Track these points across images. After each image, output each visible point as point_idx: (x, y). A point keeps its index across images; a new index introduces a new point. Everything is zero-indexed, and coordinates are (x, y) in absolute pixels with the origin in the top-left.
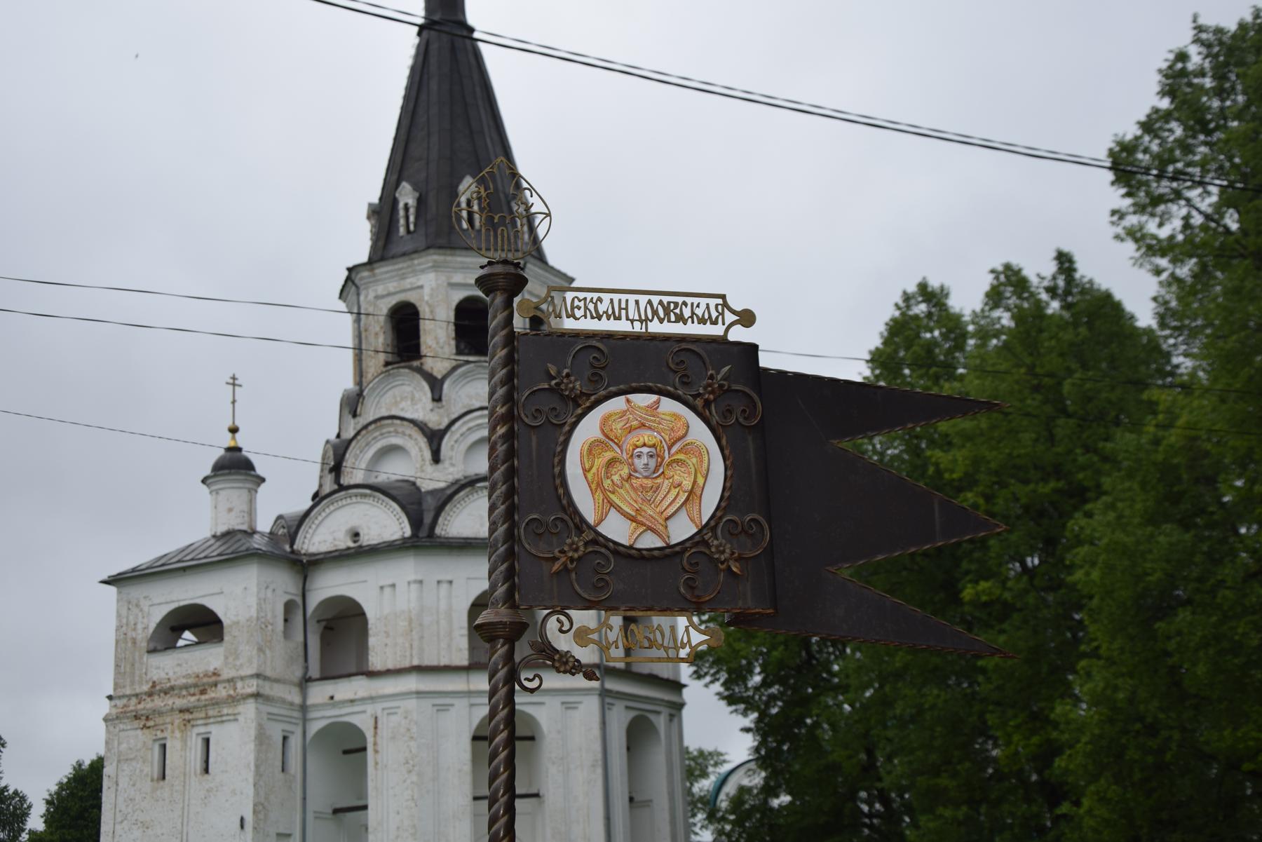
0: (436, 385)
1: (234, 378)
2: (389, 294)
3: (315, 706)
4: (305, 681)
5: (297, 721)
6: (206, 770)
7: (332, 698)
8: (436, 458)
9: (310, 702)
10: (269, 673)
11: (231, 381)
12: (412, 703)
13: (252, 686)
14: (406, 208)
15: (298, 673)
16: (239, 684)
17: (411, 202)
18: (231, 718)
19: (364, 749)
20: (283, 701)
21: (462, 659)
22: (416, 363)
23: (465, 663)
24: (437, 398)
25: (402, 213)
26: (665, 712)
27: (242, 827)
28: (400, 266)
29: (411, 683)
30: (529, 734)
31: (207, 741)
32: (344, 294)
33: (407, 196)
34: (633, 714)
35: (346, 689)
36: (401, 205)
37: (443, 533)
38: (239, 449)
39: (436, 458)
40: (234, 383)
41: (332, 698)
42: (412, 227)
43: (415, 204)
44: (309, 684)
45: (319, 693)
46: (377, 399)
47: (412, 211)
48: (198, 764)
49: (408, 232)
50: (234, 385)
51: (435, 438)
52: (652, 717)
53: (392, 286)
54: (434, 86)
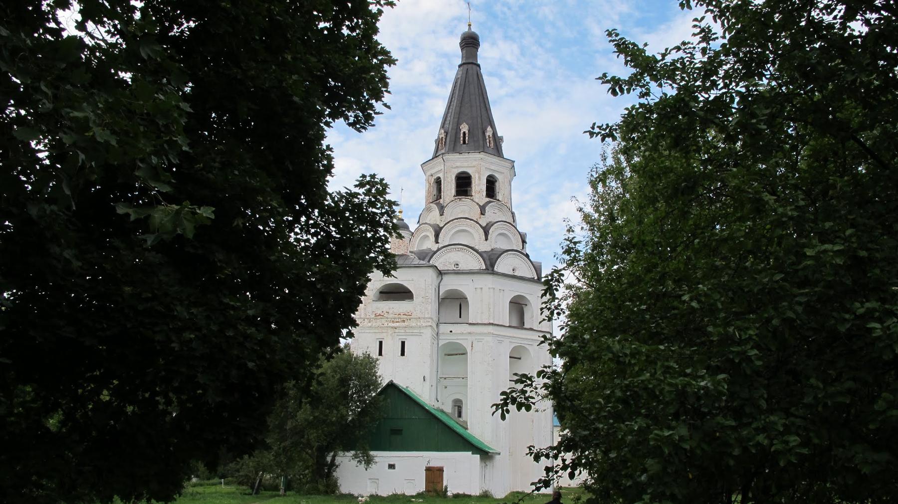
2: (457, 167)
3: (443, 333)
7: (451, 332)
9: (440, 332)
12: (490, 339)
14: (464, 133)
17: (467, 132)
23: (508, 325)
25: (462, 135)
29: (490, 329)
30: (519, 357)
32: (424, 165)
33: (464, 128)
35: (456, 329)
36: (462, 132)
41: (451, 332)
42: (467, 142)
45: (444, 328)
47: (467, 135)
49: (464, 142)
51: (486, 230)
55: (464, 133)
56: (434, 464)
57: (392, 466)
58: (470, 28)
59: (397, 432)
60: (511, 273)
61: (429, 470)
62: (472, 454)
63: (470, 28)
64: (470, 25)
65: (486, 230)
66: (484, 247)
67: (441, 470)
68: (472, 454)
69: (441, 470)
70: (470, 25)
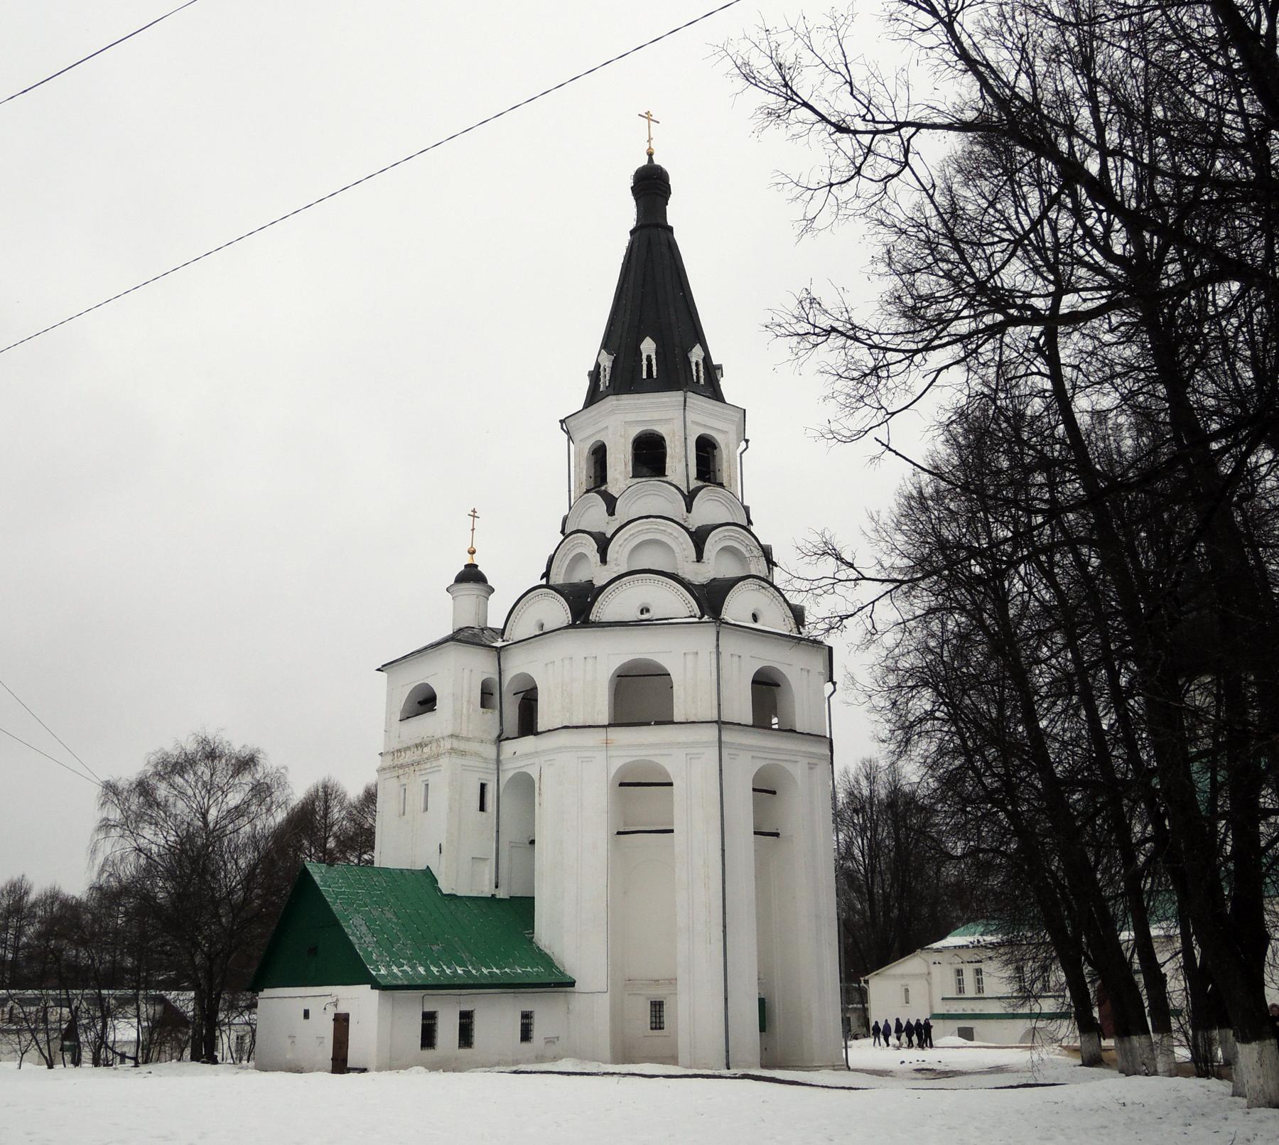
0: (611, 503)
1: (474, 511)
2: (588, 437)
4: (500, 739)
5: (492, 771)
6: (426, 809)
8: (604, 560)
10: (464, 734)
11: (472, 514)
13: (447, 744)
15: (496, 733)
18: (437, 769)
20: (477, 754)
21: (604, 718)
22: (603, 488)
23: (607, 724)
24: (611, 511)
26: (803, 762)
27: (440, 852)
28: (594, 413)
31: (427, 785)
34: (759, 764)
37: (597, 619)
38: (476, 566)
39: (604, 560)
40: (474, 514)
43: (611, 365)
44: (502, 743)
48: (422, 806)
50: (474, 516)
52: (788, 766)
54: (632, 273)
55: (649, 357)
56: (342, 1009)
58: (651, 160)
60: (634, 615)
62: (372, 988)
63: (651, 160)
64: (650, 155)
65: (699, 537)
68: (372, 988)
70: (650, 155)
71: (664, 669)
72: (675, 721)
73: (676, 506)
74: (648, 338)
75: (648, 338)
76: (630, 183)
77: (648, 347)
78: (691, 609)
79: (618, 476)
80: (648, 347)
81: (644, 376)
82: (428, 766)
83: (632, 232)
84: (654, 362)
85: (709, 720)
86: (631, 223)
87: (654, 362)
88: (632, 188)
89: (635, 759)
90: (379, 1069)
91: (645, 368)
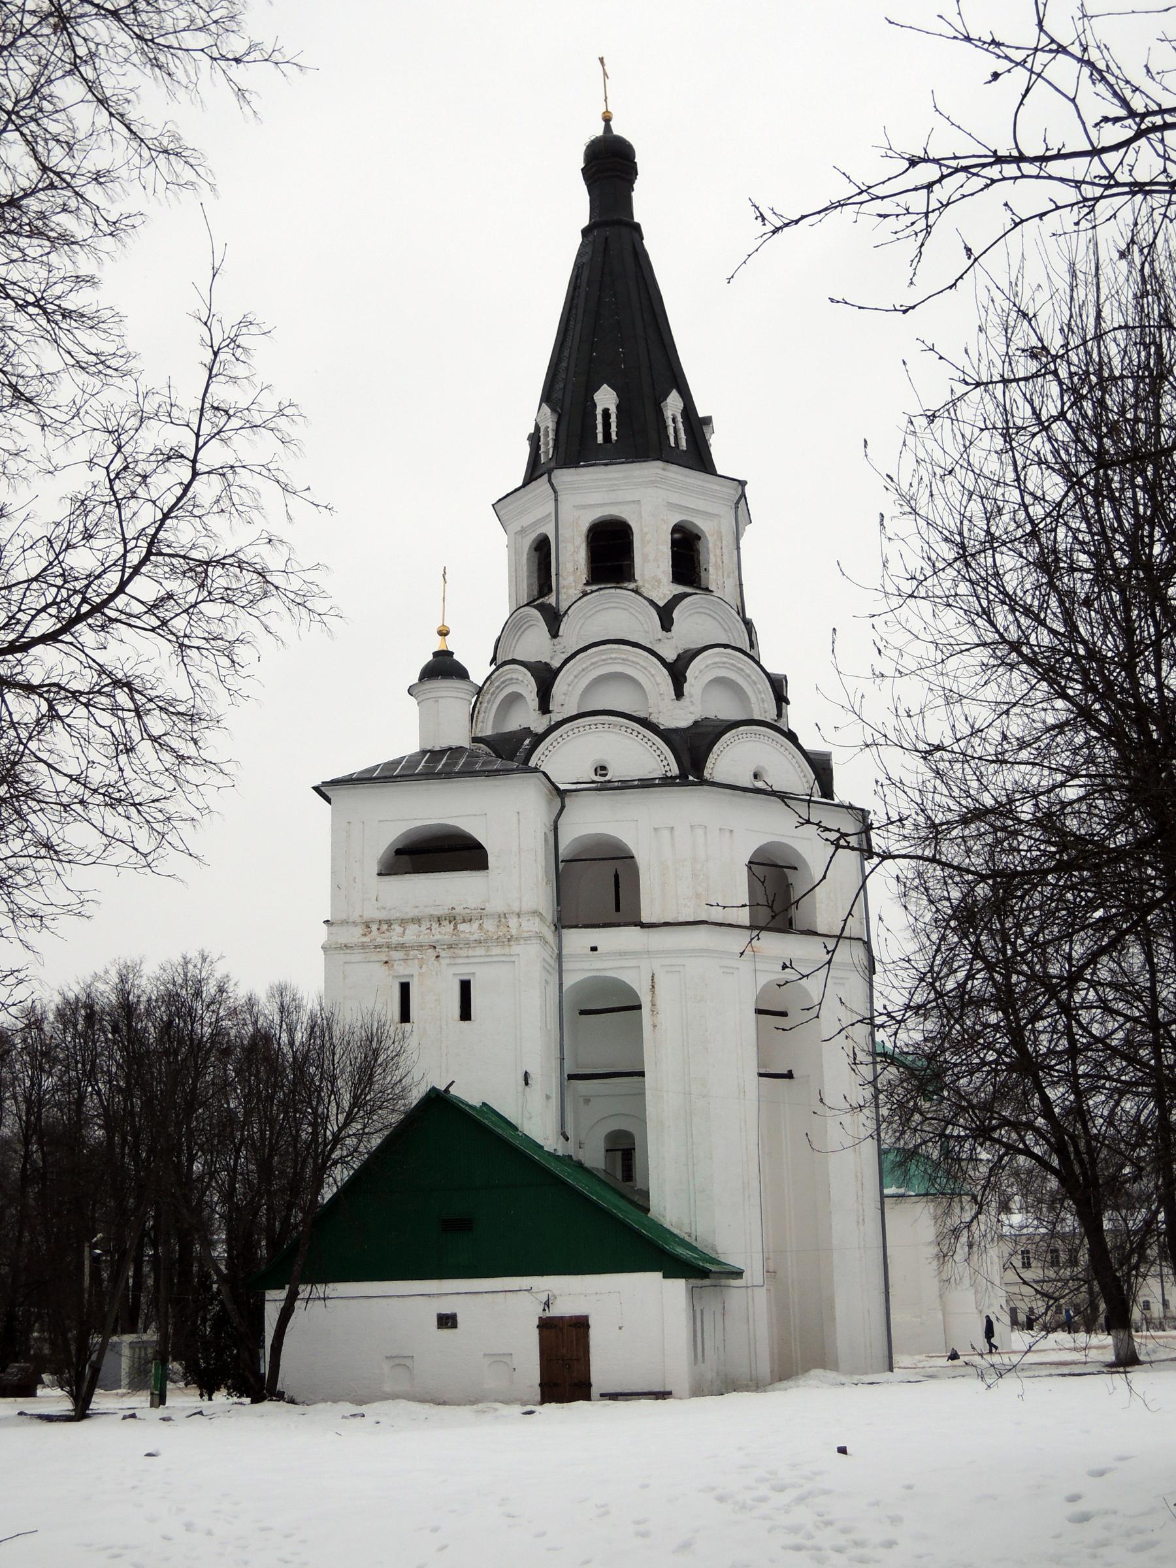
16: (513, 922)
19: (639, 1007)
27: (527, 1084)
35: (608, 939)
45: (578, 940)
46: (582, 621)
53: (595, 498)
55: (606, 413)
56: (564, 1308)
57: (447, 1321)
59: (459, 1225)
61: (548, 1326)
62: (664, 1277)
65: (677, 671)
66: (678, 716)
67: (580, 1325)
69: (580, 1325)
71: (629, 850)
72: (645, 919)
73: (646, 626)
74: (605, 386)
75: (605, 386)
76: (579, 162)
77: (606, 398)
78: (667, 768)
79: (661, 576)
80: (606, 398)
81: (600, 439)
82: (480, 951)
83: (585, 232)
84: (613, 419)
85: (691, 920)
86: (584, 219)
87: (613, 419)
88: (582, 170)
89: (590, 974)
90: (698, 1390)
91: (600, 428)
